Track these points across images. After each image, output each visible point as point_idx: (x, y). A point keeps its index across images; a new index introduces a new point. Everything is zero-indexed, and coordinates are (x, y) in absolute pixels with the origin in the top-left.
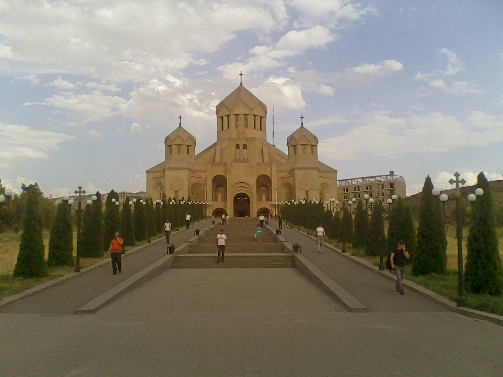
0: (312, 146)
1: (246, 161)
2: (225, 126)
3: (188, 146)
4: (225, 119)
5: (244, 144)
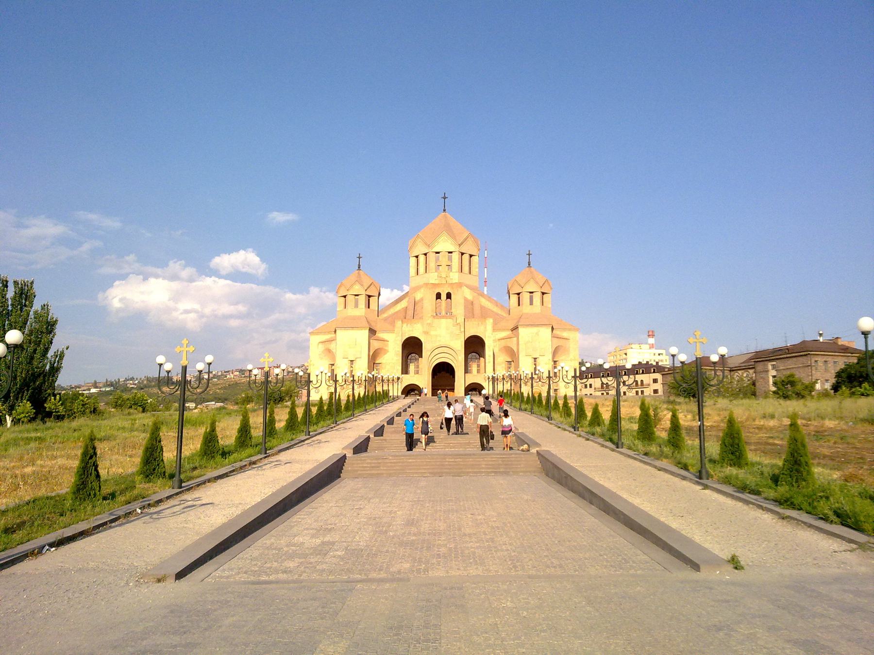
0: (543, 293)
1: (449, 314)
3: (370, 296)
4: (422, 258)
5: (447, 292)
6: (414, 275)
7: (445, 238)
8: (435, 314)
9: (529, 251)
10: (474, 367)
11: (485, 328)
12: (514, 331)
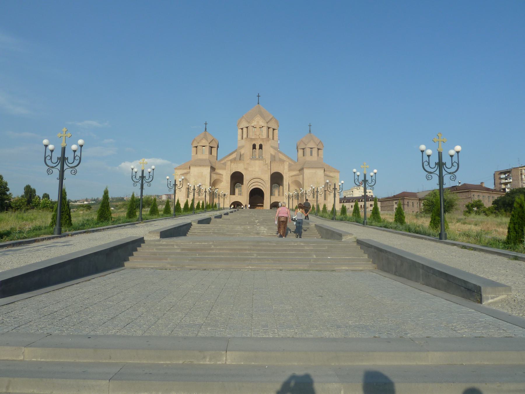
0: (319, 149)
1: (261, 158)
3: (212, 147)
4: (245, 130)
6: (240, 140)
8: (252, 158)
9: (310, 124)
10: (276, 192)
11: (284, 167)
12: (300, 171)
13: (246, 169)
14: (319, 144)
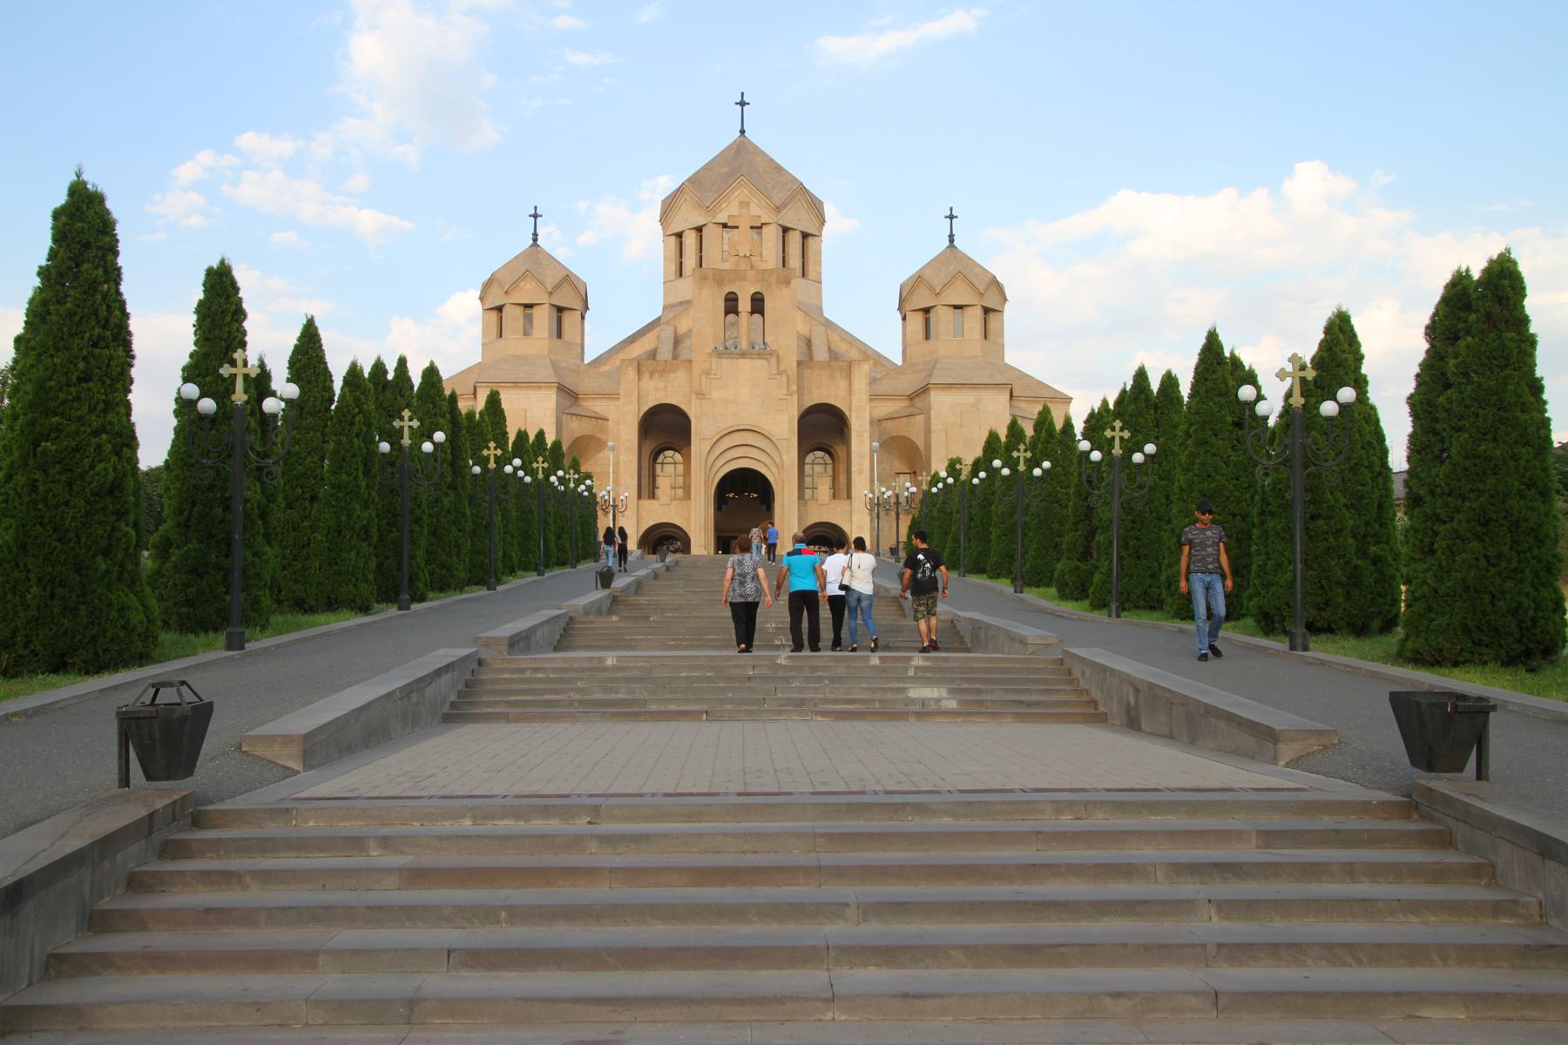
0: (987, 311)
1: (762, 351)
2: (690, 262)
3: (560, 310)
4: (690, 240)
5: (753, 291)
6: (673, 278)
7: (746, 192)
11: (850, 385)
13: (700, 395)
14: (986, 290)
